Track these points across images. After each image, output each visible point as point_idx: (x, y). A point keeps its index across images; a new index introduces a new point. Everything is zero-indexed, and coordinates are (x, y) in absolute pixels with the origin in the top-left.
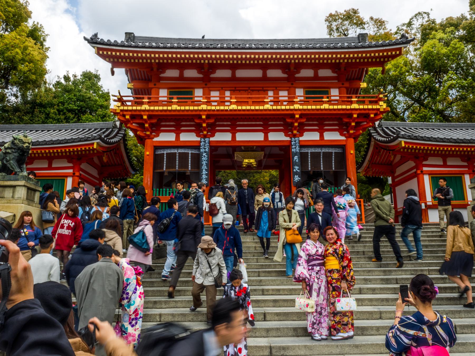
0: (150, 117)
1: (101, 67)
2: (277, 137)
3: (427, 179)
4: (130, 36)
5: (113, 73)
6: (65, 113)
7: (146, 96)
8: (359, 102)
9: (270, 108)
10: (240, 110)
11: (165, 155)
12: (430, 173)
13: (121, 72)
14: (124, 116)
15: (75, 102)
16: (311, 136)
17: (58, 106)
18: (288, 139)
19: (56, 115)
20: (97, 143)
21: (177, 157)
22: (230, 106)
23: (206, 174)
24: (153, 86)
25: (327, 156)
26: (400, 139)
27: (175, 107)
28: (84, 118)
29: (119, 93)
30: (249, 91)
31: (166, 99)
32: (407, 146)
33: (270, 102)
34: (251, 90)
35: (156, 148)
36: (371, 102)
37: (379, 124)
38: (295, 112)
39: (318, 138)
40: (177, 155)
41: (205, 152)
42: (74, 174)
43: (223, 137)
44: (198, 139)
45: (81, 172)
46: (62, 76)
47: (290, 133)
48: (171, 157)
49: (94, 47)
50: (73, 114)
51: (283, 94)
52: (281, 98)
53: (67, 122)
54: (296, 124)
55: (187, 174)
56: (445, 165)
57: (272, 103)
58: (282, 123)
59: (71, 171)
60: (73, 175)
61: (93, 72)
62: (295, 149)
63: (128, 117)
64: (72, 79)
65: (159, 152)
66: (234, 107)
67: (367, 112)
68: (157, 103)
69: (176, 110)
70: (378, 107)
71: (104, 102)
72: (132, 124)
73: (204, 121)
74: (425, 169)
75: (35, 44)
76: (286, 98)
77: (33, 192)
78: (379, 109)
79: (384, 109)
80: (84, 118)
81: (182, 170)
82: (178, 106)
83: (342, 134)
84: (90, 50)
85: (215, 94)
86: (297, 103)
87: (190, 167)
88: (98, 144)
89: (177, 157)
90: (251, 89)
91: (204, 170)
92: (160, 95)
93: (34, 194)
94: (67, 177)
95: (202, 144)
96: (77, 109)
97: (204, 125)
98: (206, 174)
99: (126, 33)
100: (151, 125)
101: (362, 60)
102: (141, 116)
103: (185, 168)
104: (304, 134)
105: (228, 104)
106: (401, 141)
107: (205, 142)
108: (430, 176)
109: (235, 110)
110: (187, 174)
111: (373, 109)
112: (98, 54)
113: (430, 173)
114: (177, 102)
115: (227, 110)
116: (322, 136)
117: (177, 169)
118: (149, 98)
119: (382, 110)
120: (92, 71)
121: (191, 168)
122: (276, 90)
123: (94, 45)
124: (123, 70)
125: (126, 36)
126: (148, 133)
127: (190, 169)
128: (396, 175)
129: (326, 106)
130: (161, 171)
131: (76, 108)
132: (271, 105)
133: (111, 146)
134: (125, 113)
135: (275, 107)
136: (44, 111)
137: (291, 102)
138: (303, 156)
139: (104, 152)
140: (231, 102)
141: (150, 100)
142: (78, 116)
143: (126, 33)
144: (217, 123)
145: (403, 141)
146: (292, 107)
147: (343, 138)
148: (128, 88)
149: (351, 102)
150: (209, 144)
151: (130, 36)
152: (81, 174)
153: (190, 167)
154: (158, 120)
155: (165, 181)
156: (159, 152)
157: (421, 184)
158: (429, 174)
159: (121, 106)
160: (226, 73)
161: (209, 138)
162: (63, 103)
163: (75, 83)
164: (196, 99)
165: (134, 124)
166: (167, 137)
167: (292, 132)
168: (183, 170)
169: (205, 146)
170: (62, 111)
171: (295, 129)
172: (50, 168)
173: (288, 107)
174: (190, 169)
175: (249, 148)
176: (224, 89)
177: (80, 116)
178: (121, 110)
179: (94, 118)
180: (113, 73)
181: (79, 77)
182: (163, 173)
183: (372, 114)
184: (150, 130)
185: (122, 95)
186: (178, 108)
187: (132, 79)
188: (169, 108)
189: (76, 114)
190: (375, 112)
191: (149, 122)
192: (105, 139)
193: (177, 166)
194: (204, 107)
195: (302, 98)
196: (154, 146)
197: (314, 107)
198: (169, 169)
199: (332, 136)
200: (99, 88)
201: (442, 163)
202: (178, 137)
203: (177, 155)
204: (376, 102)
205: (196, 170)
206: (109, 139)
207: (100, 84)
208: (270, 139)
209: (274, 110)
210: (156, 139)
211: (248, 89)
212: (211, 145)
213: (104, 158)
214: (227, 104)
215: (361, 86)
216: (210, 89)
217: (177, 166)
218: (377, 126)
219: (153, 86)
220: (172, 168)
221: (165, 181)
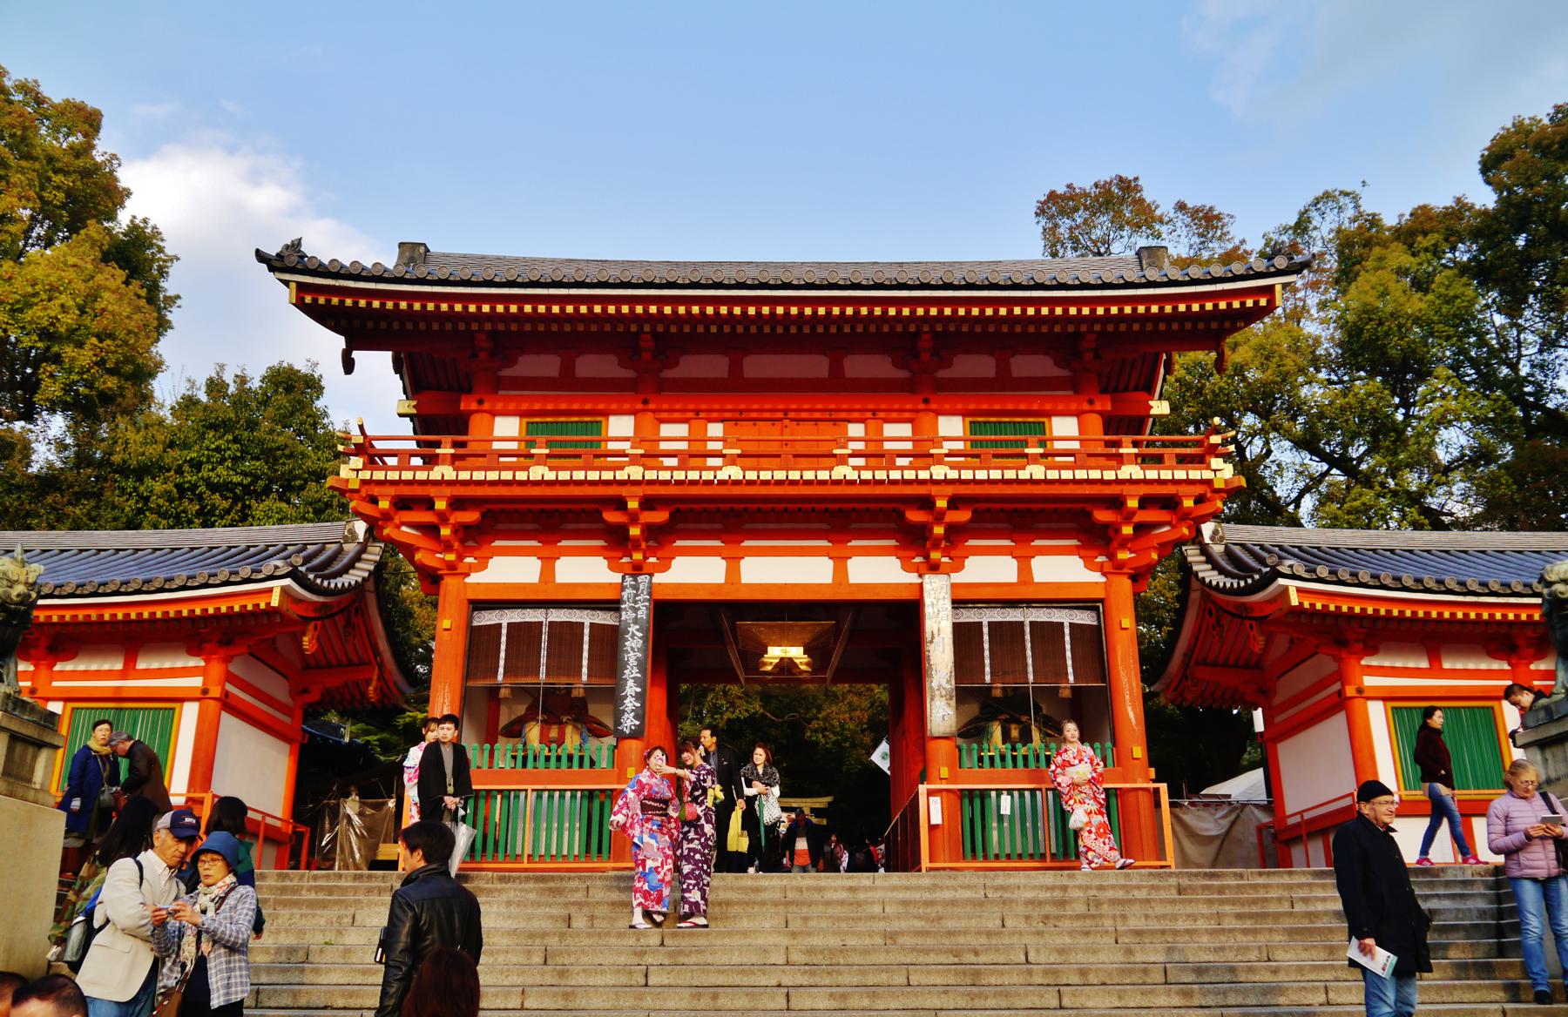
0: (457, 504)
1: (317, 348)
2: (876, 570)
3: (1377, 713)
4: (413, 252)
5: (349, 366)
6: (201, 494)
7: (447, 439)
8: (1145, 460)
9: (852, 475)
10: (751, 483)
11: (504, 631)
12: (1387, 697)
13: (377, 364)
14: (374, 500)
15: (235, 459)
17: (179, 471)
18: (913, 578)
19: (171, 500)
20: (284, 590)
21: (545, 637)
22: (720, 468)
23: (638, 697)
24: (474, 406)
25: (1047, 634)
26: (1281, 581)
27: (538, 472)
28: (259, 508)
29: (361, 427)
30: (786, 422)
31: (514, 446)
32: (1306, 605)
33: (851, 456)
34: (792, 420)
36: (1183, 460)
37: (1215, 532)
38: (934, 490)
40: (545, 629)
41: (636, 621)
42: (205, 691)
43: (695, 571)
44: (616, 578)
45: (229, 687)
46: (201, 382)
47: (918, 560)
48: (524, 635)
49: (286, 283)
50: (226, 499)
51: (897, 433)
52: (888, 446)
53: (205, 525)
54: (939, 530)
55: (575, 694)
56: (1435, 670)
57: (861, 462)
58: (893, 525)
59: (197, 682)
60: (202, 696)
61: (301, 366)
63: (384, 504)
64: (232, 389)
65: (486, 619)
66: (735, 472)
67: (1171, 490)
68: (491, 459)
69: (542, 483)
70: (1207, 475)
71: (328, 460)
72: (398, 527)
73: (634, 518)
74: (1369, 681)
75: (127, 283)
76: (908, 446)
77: (31, 750)
78: (1209, 482)
79: (1226, 481)
80: (258, 514)
81: (561, 681)
82: (551, 469)
83: (1090, 566)
84: (277, 293)
85: (674, 433)
86: (939, 460)
87: (585, 670)
88: (285, 591)
89: (545, 637)
90: (792, 415)
91: (630, 683)
92: (497, 433)
93: (35, 758)
94: (182, 700)
95: (625, 594)
96: (240, 484)
97: (635, 531)
98: (638, 697)
99: (401, 245)
101: (1149, 327)
102: (428, 503)
103: (569, 676)
104: (968, 562)
105: (717, 462)
106: (1286, 589)
107: (636, 588)
108: (1390, 704)
109: (737, 483)
110: (575, 694)
111: (1189, 482)
112: (300, 305)
113: (1387, 697)
114: (548, 456)
115: (709, 483)
117: (543, 676)
119: (1218, 485)
120: (297, 367)
121: (589, 676)
122: (874, 417)
123: (287, 277)
124: (385, 358)
125: (401, 254)
126: (451, 557)
127: (584, 678)
128: (1276, 701)
129: (1037, 471)
130: (487, 683)
131: (237, 479)
132: (854, 468)
133: (321, 599)
134: (376, 491)
135: (867, 475)
136: (136, 490)
137: (922, 457)
138: (965, 636)
139: (306, 620)
140: (723, 456)
141: (461, 451)
142: (245, 507)
143: (401, 245)
144: (680, 526)
145: (1293, 585)
146: (924, 475)
147: (1097, 577)
148: (401, 415)
149: (1120, 460)
150: (650, 594)
151: (413, 252)
152: (227, 694)
153: (585, 670)
154: (483, 515)
155: (504, 720)
156: (486, 619)
157: (1359, 733)
158: (1385, 699)
159: (364, 468)
160: (714, 366)
161: (651, 575)
162: (196, 465)
163: (242, 399)
164: (612, 446)
165: (404, 529)
166: (511, 569)
167: (927, 557)
168: (564, 680)
169: (636, 602)
170: (194, 487)
171: (936, 547)
173: (910, 475)
174: (584, 678)
175: (784, 611)
176: (702, 415)
177: (250, 507)
178: (364, 482)
179: (290, 511)
180: (349, 366)
181: (255, 384)
182: (494, 690)
183: (1188, 496)
184: (456, 545)
185: (369, 432)
186: (550, 476)
187: (415, 386)
188: (521, 476)
189: (236, 499)
190: (1198, 490)
191: (452, 520)
192: (311, 576)
193: (543, 669)
194: (636, 472)
195: (959, 446)
196: (471, 602)
197: (996, 474)
198: (516, 676)
199: (1063, 569)
200: (316, 419)
201: (1424, 664)
203: (545, 629)
204: (1200, 460)
205: (604, 683)
206: (324, 578)
207: (319, 404)
209: (864, 482)
210: (474, 578)
211: (780, 415)
212: (656, 597)
213: (306, 639)
214: (711, 462)
215: (1153, 412)
216: (664, 415)
217: (543, 669)
218: (1207, 540)
219: (474, 406)
220: (526, 676)
221: (504, 720)
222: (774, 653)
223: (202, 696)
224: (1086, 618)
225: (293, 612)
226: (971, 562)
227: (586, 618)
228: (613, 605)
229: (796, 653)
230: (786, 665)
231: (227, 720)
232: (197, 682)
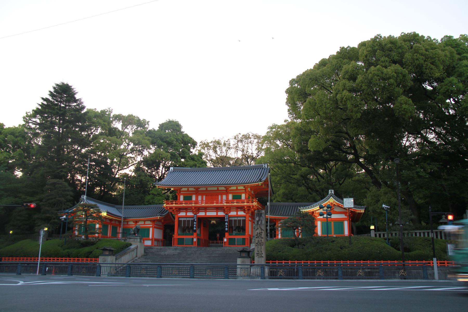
2: (221, 214)
16: (233, 213)
35: (179, 218)
43: (202, 214)
48: (184, 221)
59: (151, 225)
60: (152, 227)
100: (177, 211)
116: (237, 213)
156: (180, 219)
166: (182, 214)
172: (145, 224)
199: (241, 213)
202: (186, 214)
222: (212, 222)
223: (152, 227)
224: (244, 218)
226: (231, 212)
227: (190, 219)
232: (151, 225)
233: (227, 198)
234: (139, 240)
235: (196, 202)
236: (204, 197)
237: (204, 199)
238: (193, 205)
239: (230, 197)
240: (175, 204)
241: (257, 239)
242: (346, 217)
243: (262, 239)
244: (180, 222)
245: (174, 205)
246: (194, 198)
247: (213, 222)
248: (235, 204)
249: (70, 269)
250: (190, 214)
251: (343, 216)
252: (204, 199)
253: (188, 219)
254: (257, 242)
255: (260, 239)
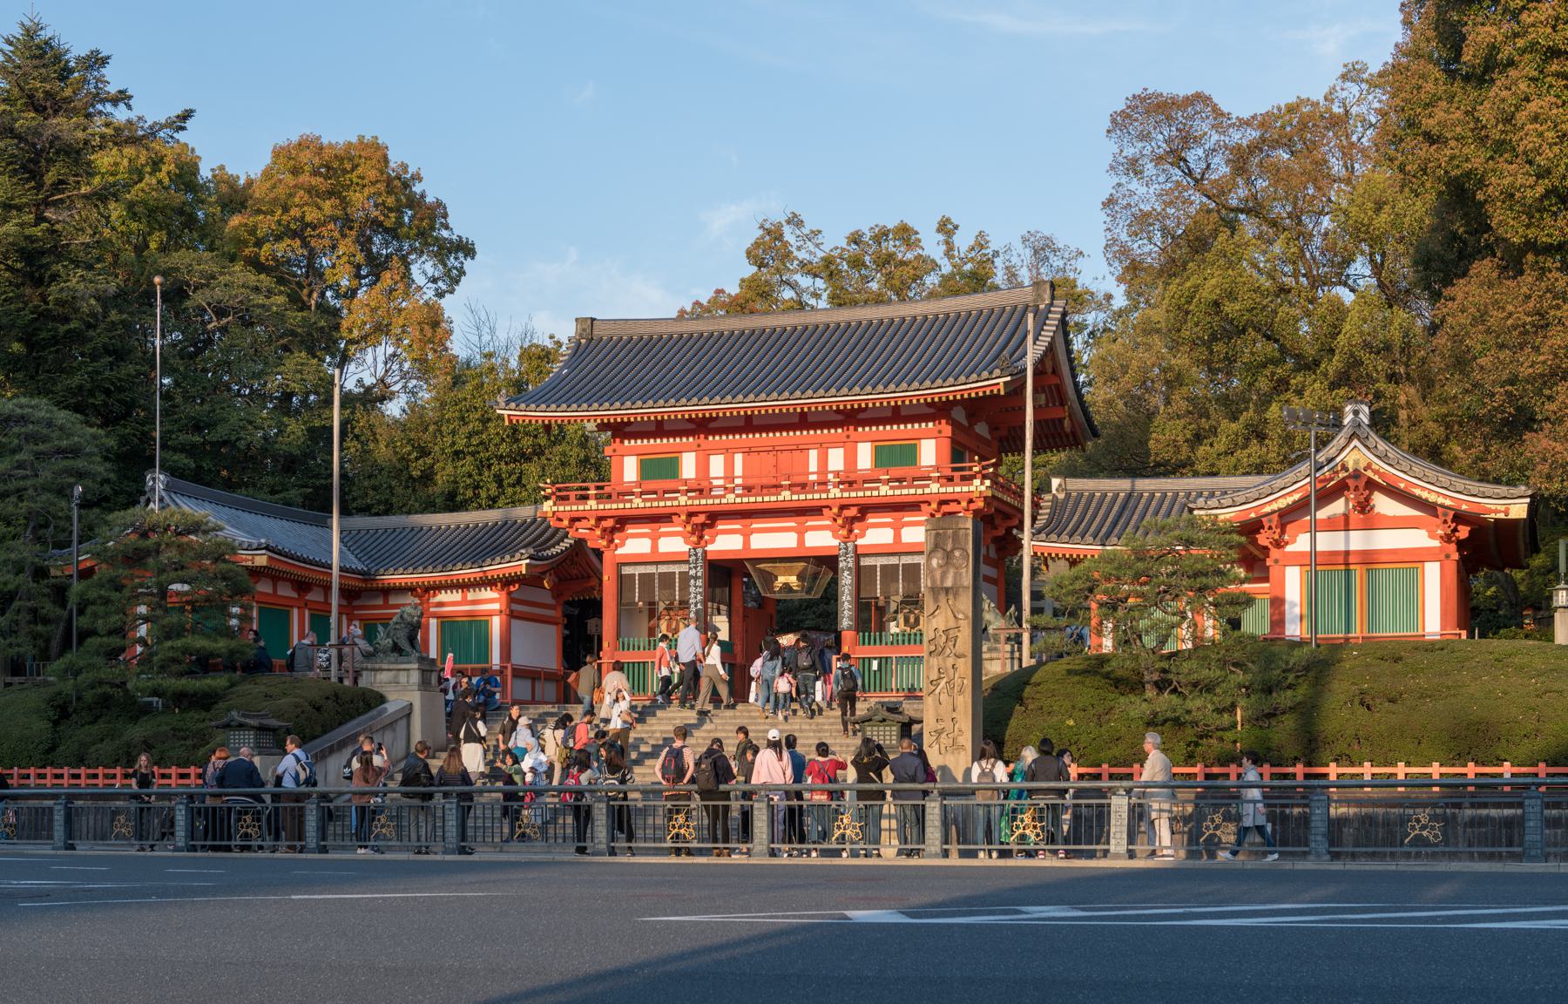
0: (600, 519)
2: (821, 538)
7: (591, 485)
35: (620, 565)
39: (890, 540)
43: (726, 543)
48: (647, 579)
62: (846, 563)
118: (598, 488)
156: (627, 570)
166: (635, 544)
172: (464, 602)
208: (808, 543)
210: (620, 551)
222: (782, 579)
225: (536, 572)
227: (676, 569)
228: (687, 562)
229: (793, 580)
230: (787, 587)
231: (516, 623)
232: (497, 606)
233: (851, 459)
234: (415, 677)
235: (701, 488)
236: (738, 459)
237: (738, 471)
238: (683, 500)
239: (865, 456)
240: (598, 498)
241: (934, 661)
242: (1436, 543)
243: (961, 662)
244: (623, 581)
245: (592, 504)
246: (688, 467)
247: (788, 579)
248: (884, 490)
249: (59, 818)
250: (674, 543)
251: (1418, 539)
252: (738, 471)
253: (663, 569)
254: (934, 676)
255: (950, 661)
